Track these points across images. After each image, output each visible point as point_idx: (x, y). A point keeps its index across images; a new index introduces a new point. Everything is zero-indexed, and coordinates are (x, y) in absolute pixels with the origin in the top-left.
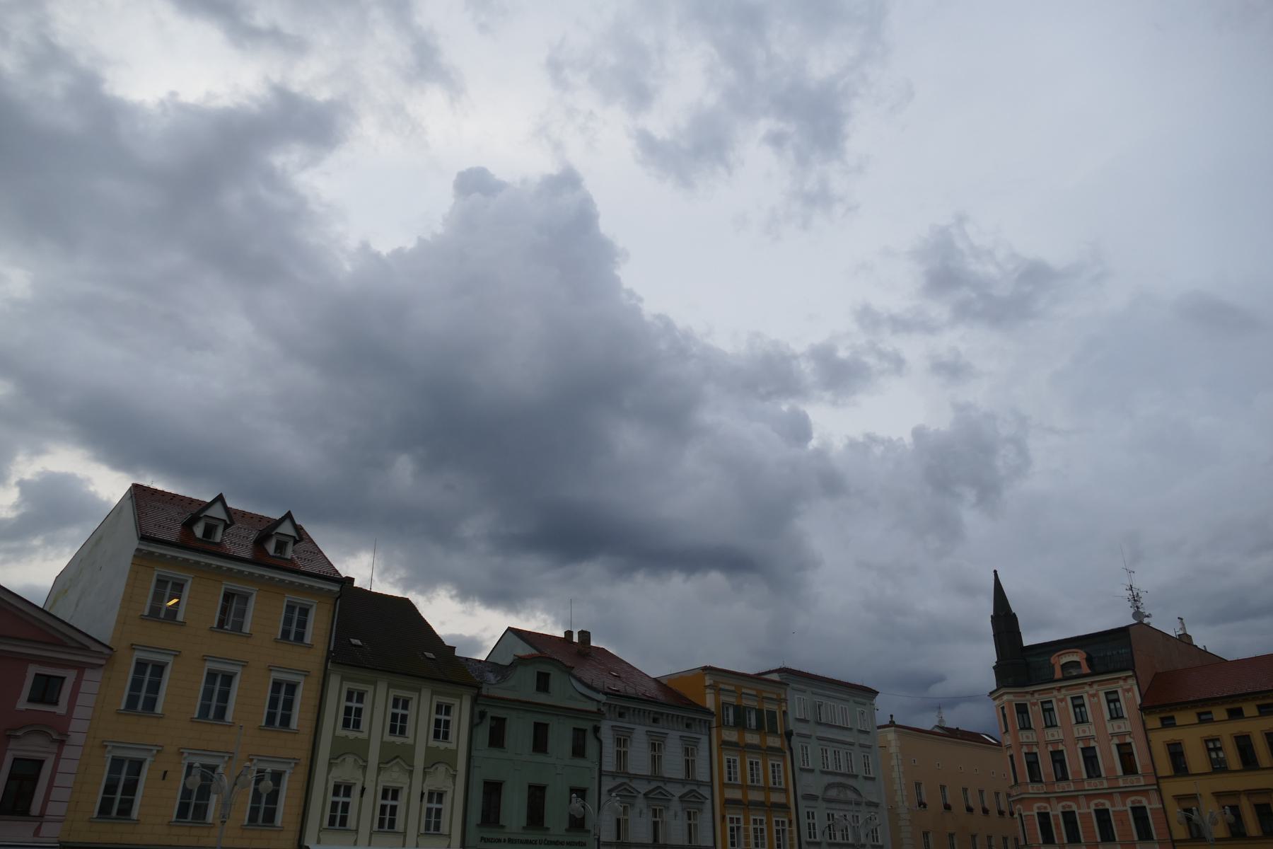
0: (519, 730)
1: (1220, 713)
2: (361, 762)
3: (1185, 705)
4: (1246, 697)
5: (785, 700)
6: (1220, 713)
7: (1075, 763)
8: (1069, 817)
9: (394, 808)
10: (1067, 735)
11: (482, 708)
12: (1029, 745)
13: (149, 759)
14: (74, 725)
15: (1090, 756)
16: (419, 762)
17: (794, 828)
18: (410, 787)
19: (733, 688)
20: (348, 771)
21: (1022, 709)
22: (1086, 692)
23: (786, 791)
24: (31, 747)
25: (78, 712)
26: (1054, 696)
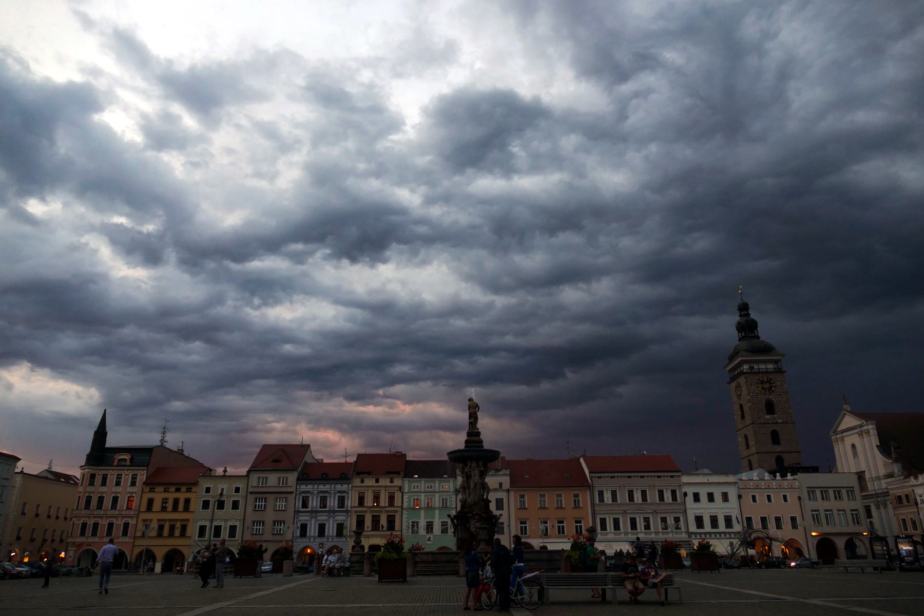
1: (172, 489)
3: (160, 484)
4: (184, 484)
6: (172, 489)
7: (108, 503)
8: (96, 525)
10: (108, 491)
12: (90, 492)
15: (115, 500)
21: (93, 477)
22: (124, 473)
26: (109, 473)
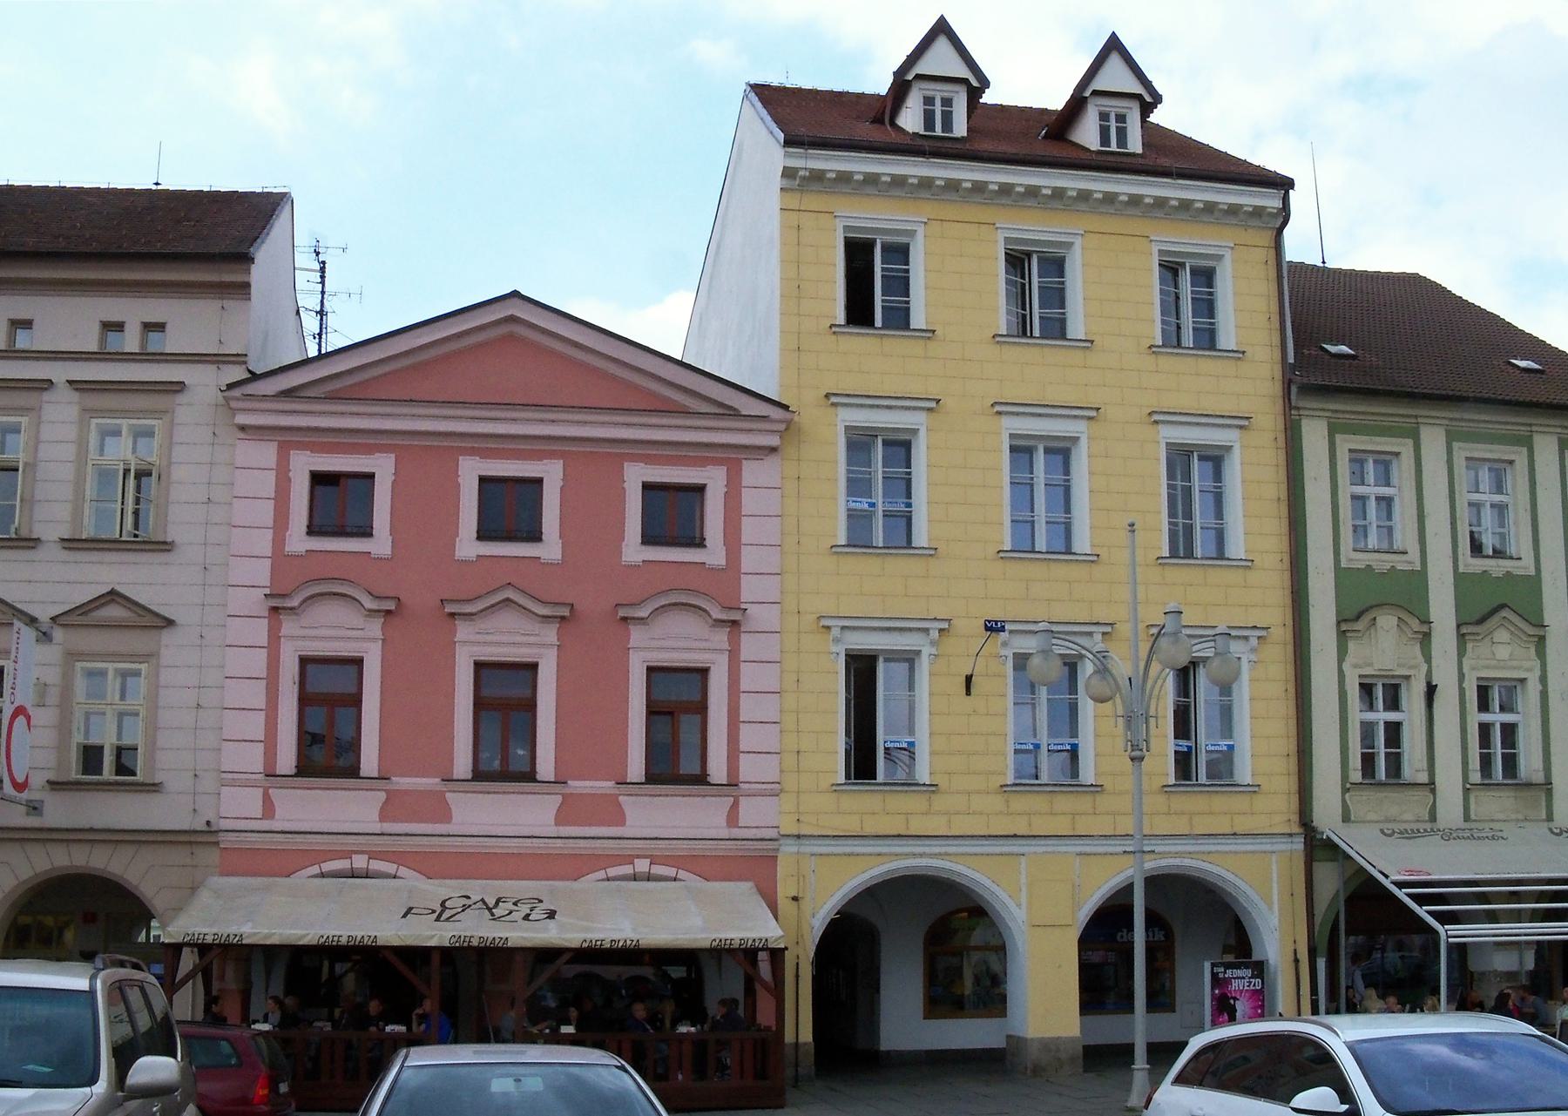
2: (1415, 624)
9: (1509, 731)
13: (926, 651)
14: (750, 589)
18: (1543, 679)
20: (1384, 647)
25: (750, 559)
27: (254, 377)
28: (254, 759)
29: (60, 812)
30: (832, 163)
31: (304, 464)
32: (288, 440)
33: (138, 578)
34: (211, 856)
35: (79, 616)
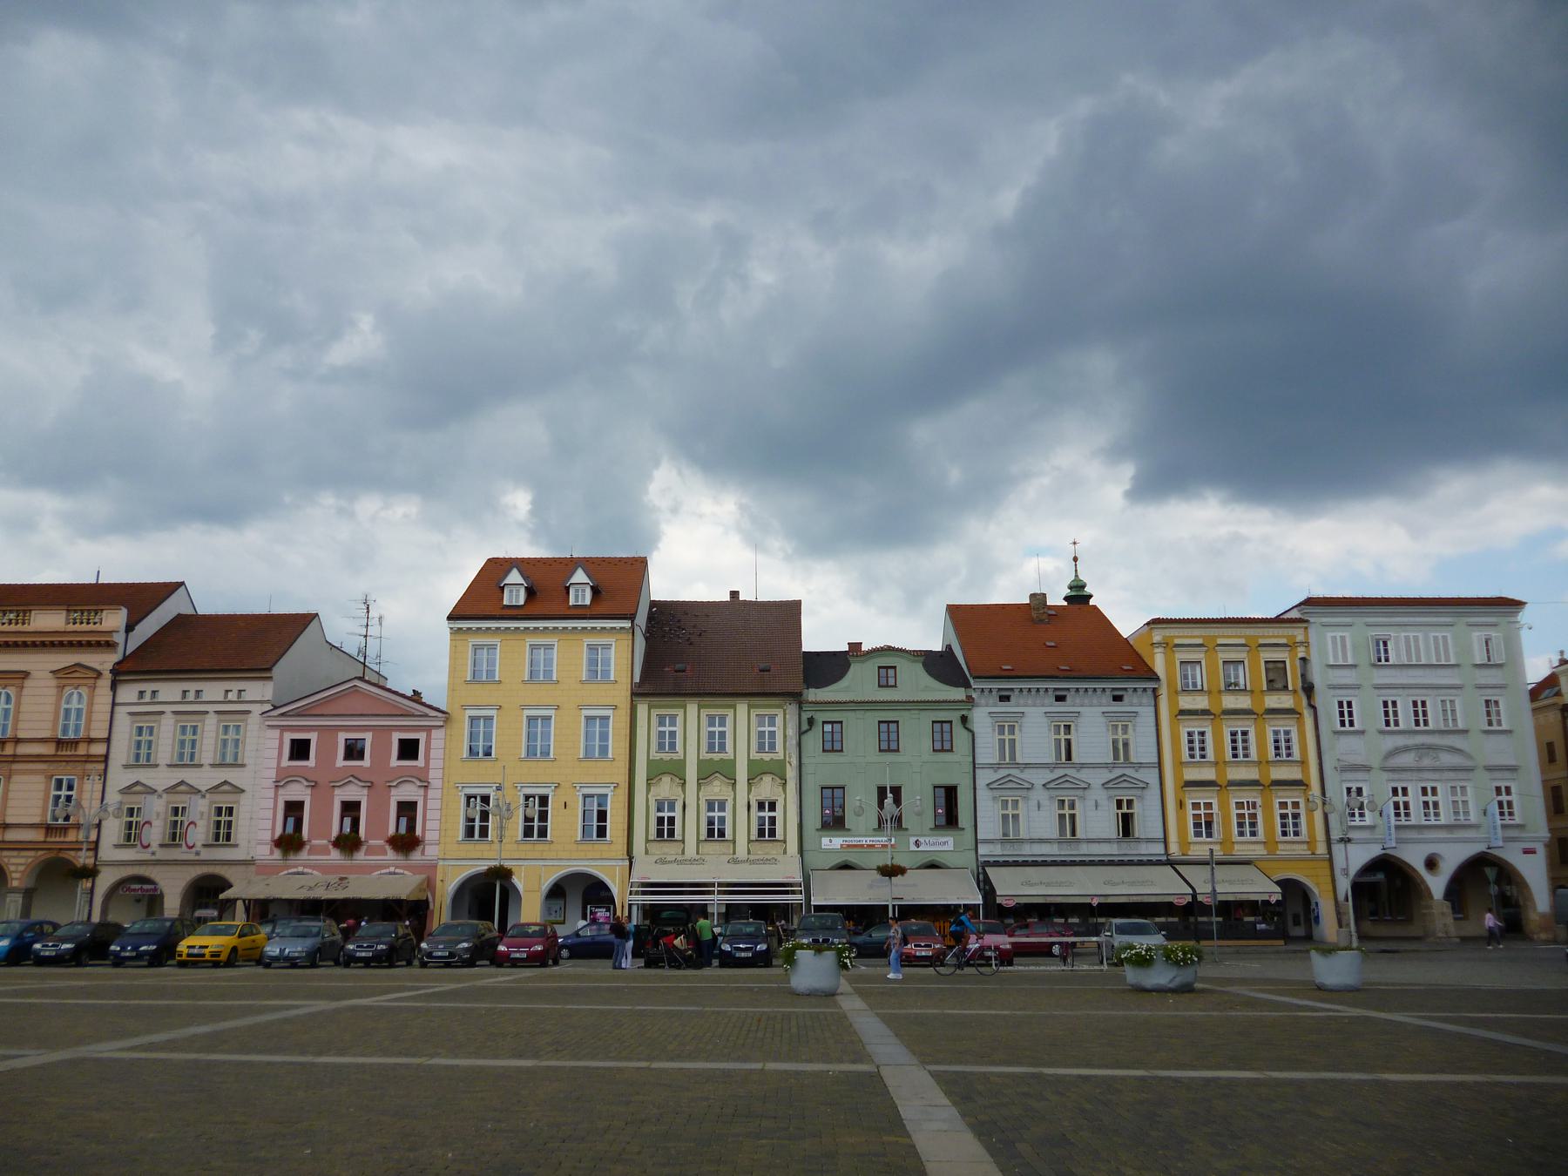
0: (860, 732)
5: (1306, 644)
11: (809, 715)
14: (432, 774)
16: (742, 774)
17: (1318, 816)
19: (1200, 641)
23: (1303, 763)
24: (408, 792)
25: (432, 764)
27: (275, 708)
28: (267, 836)
29: (206, 854)
30: (465, 625)
31: (289, 736)
32: (283, 729)
33: (232, 775)
34: (253, 868)
35: (215, 789)
